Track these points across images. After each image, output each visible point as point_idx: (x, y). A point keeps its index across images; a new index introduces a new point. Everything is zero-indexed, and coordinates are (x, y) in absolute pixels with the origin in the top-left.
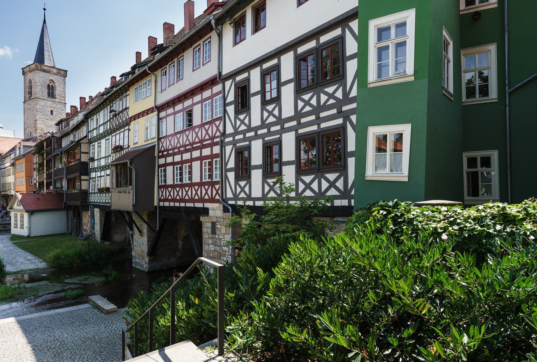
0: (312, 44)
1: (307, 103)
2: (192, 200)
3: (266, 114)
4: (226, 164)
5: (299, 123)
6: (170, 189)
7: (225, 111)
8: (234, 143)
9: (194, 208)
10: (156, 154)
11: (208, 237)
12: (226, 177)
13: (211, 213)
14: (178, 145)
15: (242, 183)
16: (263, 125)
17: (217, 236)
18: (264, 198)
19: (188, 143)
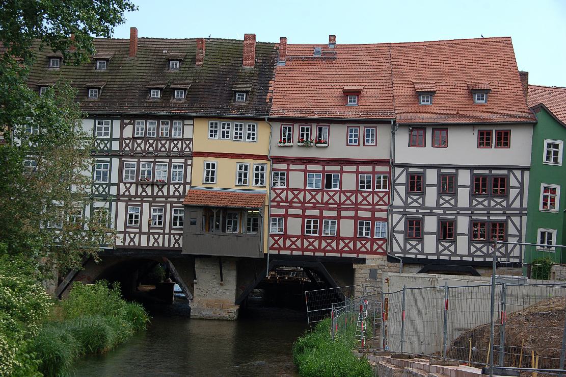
0: (487, 172)
1: (481, 203)
2: (337, 250)
3: (441, 201)
4: (393, 228)
5: (473, 213)
6: (294, 239)
7: (395, 189)
8: (404, 214)
9: (341, 257)
10: (267, 203)
11: (364, 281)
12: (393, 237)
13: (367, 261)
14: (313, 201)
15: (414, 243)
16: (438, 206)
17: (377, 280)
18: (438, 253)
19: (331, 201)
